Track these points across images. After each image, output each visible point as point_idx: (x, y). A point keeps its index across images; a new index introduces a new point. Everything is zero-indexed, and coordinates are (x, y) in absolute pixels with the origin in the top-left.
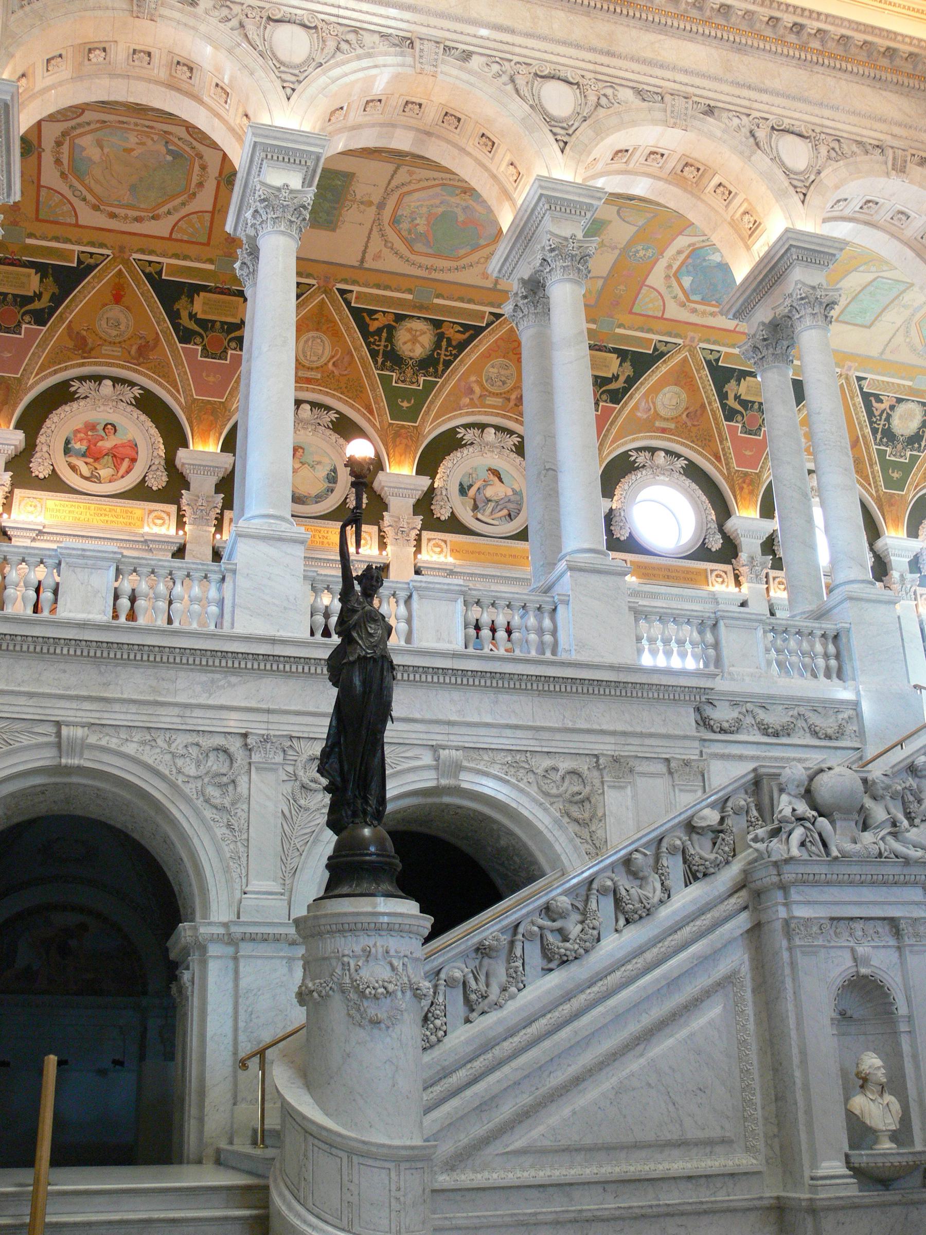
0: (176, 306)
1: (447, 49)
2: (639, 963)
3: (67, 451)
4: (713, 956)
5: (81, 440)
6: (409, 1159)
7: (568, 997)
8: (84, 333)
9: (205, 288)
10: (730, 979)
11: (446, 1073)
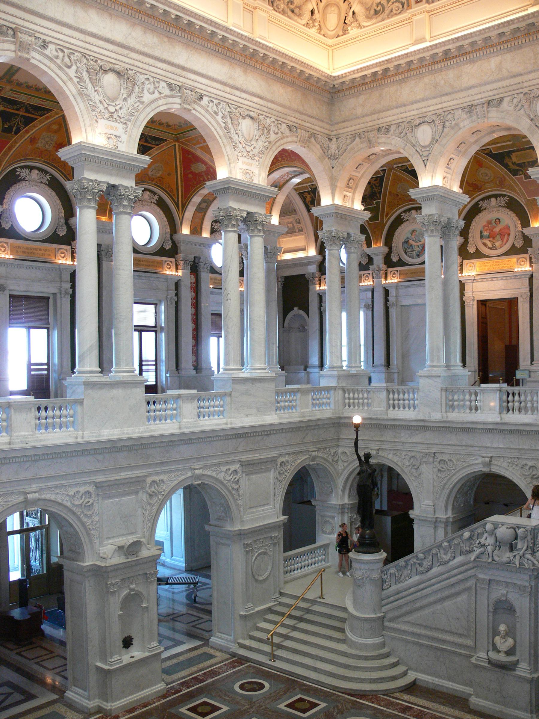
0: (505, 162)
1: (489, 103)
2: (438, 579)
3: (482, 237)
4: (466, 579)
5: (486, 230)
6: (365, 620)
7: (420, 583)
8: (475, 182)
9: (513, 151)
10: (469, 589)
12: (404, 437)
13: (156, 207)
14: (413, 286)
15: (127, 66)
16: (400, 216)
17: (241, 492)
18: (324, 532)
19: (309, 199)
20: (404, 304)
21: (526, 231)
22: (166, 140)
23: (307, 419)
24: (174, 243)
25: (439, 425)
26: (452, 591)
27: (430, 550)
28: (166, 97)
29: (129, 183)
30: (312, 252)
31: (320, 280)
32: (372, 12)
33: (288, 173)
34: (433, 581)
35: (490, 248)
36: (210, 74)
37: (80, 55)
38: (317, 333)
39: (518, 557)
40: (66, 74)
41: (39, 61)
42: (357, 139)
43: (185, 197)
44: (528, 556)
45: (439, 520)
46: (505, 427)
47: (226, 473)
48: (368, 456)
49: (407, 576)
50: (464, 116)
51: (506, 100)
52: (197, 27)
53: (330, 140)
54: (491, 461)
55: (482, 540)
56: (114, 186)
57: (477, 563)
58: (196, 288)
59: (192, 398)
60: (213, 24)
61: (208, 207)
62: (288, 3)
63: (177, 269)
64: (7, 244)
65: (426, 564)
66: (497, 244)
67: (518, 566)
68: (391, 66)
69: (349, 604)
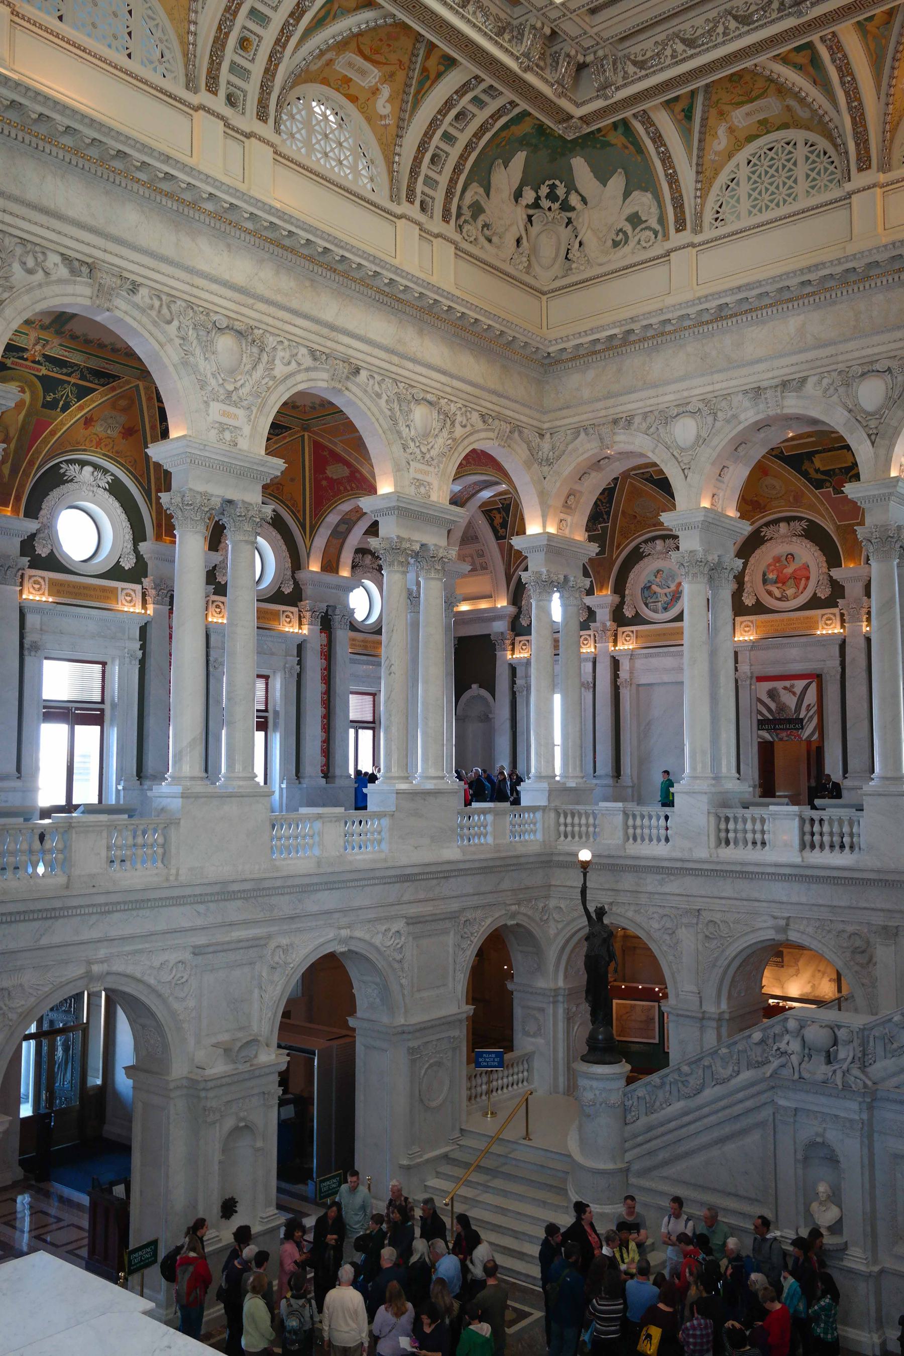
1: (784, 384)
3: (765, 581)
4: (758, 1108)
9: (817, 452)
11: (636, 1136)
12: (651, 883)
13: (271, 529)
14: (657, 655)
15: (252, 323)
16: (637, 548)
17: (406, 966)
18: (527, 1034)
19: (498, 520)
20: (642, 681)
21: (835, 573)
22: (290, 429)
23: (503, 854)
24: (296, 584)
25: (705, 866)
26: (737, 1126)
27: (700, 1059)
28: (307, 370)
29: (254, 496)
30: (502, 603)
31: (513, 644)
32: (610, 243)
33: (475, 483)
34: (706, 1110)
35: (779, 599)
36: (372, 336)
37: (184, 304)
38: (507, 725)
39: (839, 1074)
40: (164, 332)
41: (126, 312)
42: (582, 435)
43: (316, 515)
44: (856, 1072)
45: (707, 1016)
46: (809, 872)
47: (384, 934)
48: (601, 912)
49: (666, 1102)
50: (747, 403)
51: (811, 381)
52: (354, 266)
53: (542, 436)
54: (787, 925)
55: (783, 1046)
56: (230, 502)
57: (774, 1083)
58: (328, 654)
59: (338, 819)
60: (377, 261)
61: (349, 531)
62: (483, 227)
63: (300, 624)
64: (43, 578)
65: (693, 1082)
66: (790, 592)
67: (840, 1087)
68: (636, 326)
69: (573, 1146)
